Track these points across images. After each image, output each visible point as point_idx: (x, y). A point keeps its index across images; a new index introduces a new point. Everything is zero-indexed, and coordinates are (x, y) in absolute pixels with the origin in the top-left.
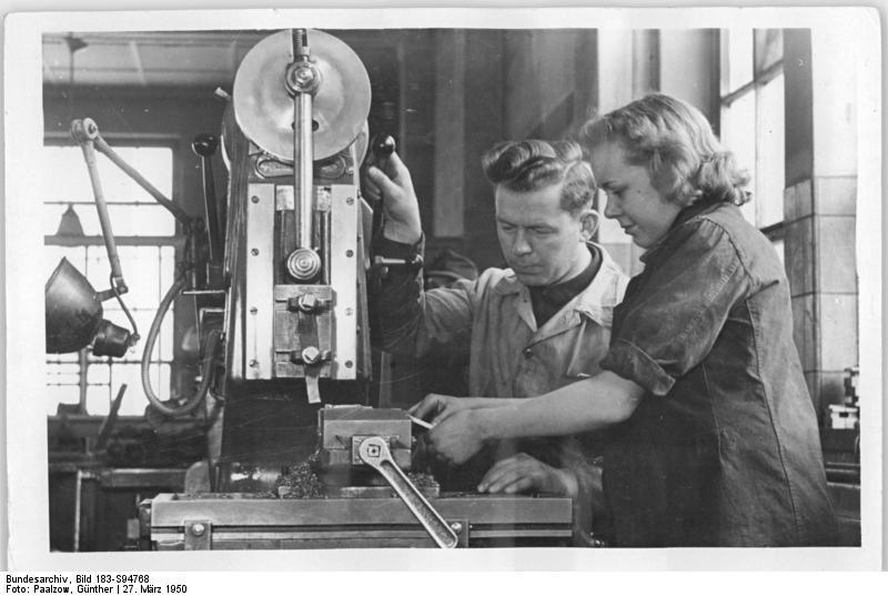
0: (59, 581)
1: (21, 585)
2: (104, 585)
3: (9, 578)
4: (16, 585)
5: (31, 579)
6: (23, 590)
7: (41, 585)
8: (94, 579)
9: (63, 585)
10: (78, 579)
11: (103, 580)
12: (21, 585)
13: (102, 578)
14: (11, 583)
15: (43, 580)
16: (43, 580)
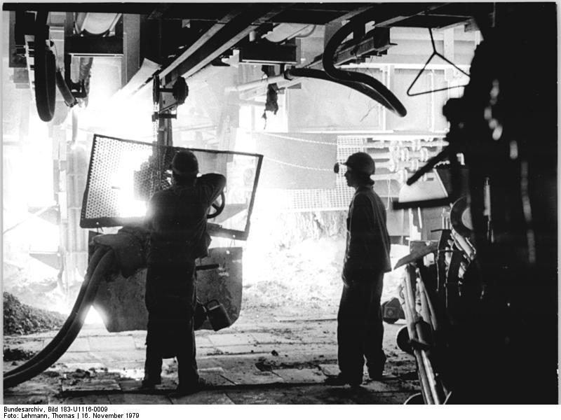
0: (38, 410)
1: (13, 413)
2: (67, 413)
3: (5, 409)
4: (10, 413)
5: (20, 410)
6: (15, 417)
7: (27, 413)
8: (59, 409)
9: (40, 413)
10: (50, 409)
11: (65, 409)
12: (13, 413)
13: (65, 409)
14: (7, 412)
15: (27, 410)
16: (27, 410)
